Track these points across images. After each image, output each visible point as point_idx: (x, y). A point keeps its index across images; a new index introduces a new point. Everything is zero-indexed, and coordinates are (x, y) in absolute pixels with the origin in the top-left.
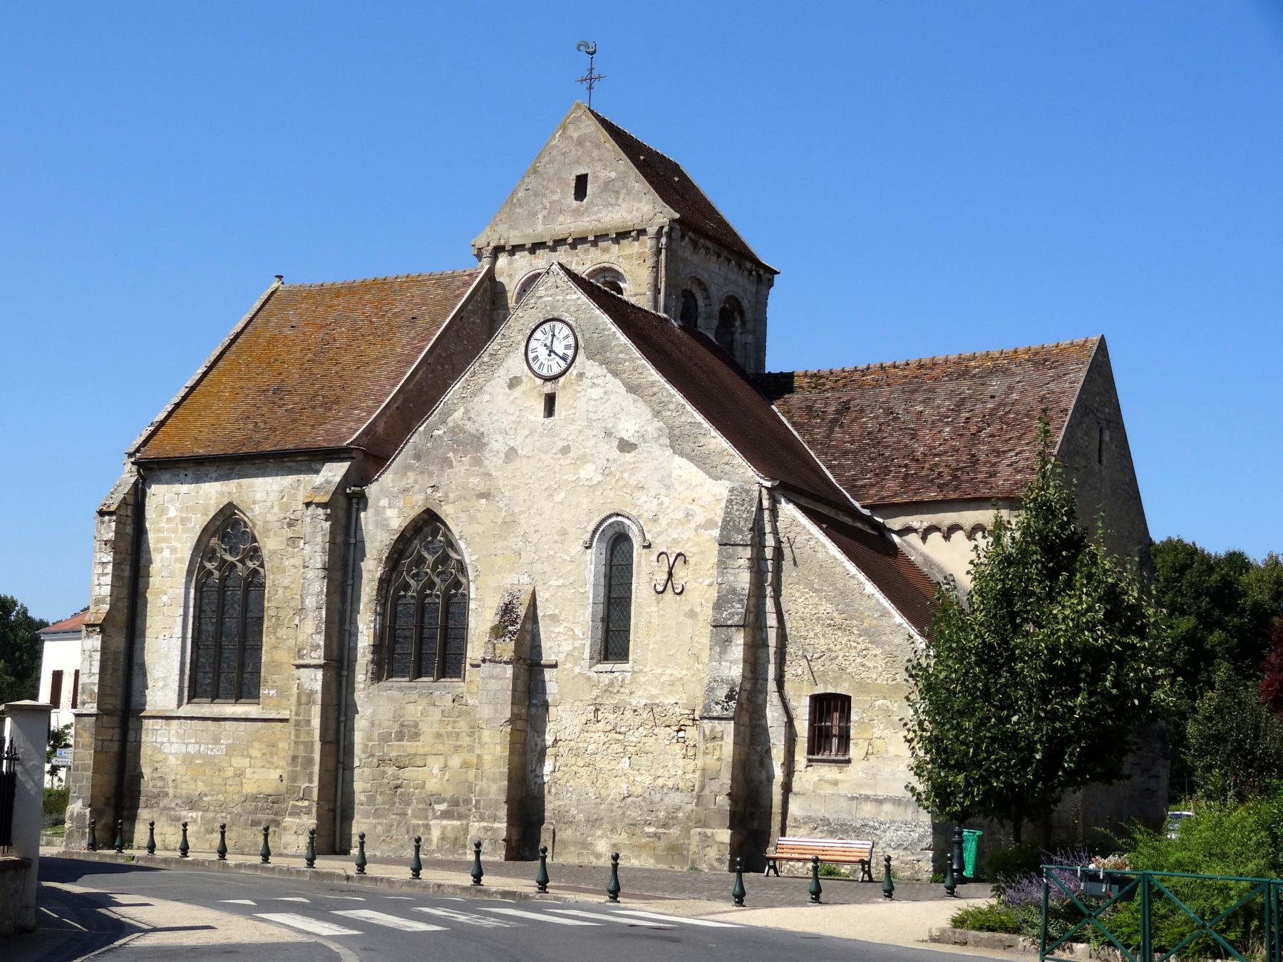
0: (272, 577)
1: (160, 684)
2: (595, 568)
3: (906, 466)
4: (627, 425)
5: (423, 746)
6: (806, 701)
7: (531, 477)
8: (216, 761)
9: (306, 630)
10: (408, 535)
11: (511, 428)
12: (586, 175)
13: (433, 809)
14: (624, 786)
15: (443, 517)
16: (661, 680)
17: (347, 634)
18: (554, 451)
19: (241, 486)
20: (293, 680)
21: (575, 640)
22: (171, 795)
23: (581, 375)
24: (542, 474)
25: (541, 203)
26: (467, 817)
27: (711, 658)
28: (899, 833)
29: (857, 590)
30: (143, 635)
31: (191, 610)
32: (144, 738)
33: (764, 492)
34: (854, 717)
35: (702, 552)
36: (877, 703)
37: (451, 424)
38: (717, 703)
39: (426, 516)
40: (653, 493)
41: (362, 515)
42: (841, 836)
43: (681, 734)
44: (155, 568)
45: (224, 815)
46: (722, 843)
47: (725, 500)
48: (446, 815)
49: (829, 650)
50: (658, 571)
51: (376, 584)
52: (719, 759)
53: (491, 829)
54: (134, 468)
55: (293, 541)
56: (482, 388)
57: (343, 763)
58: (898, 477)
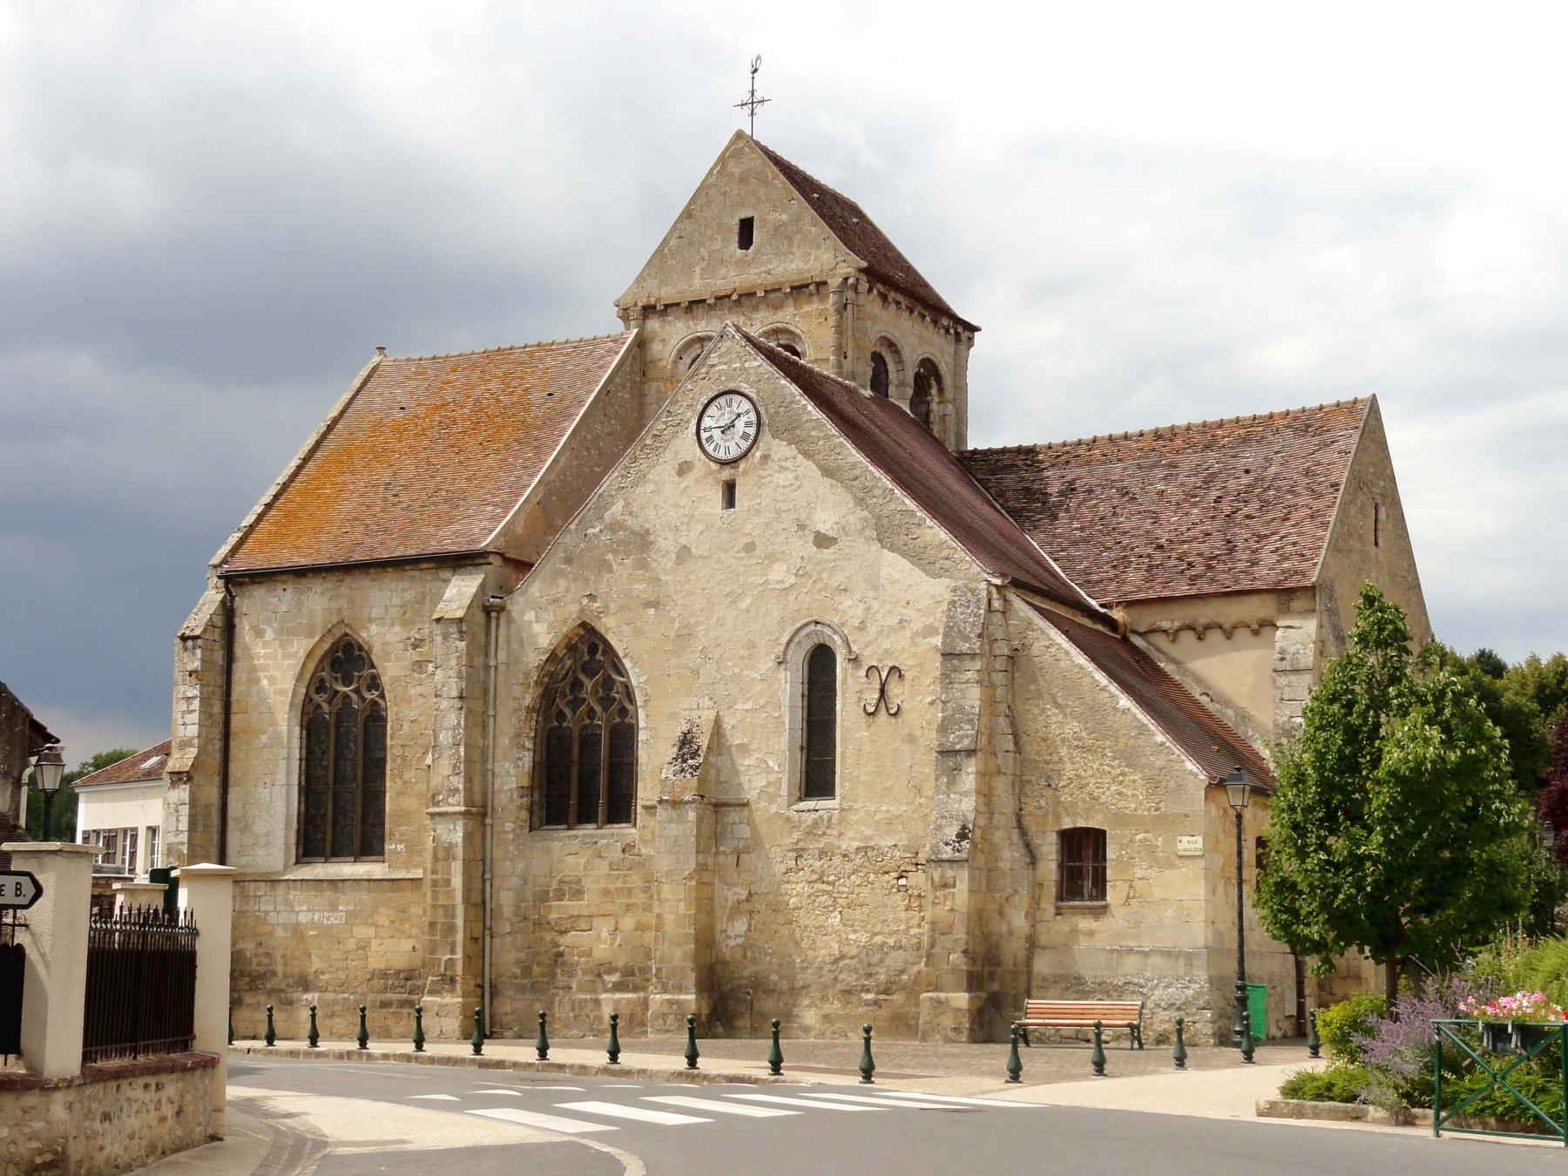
2: (791, 687)
3: (1149, 556)
4: (825, 516)
5: (588, 906)
6: (1053, 838)
7: (708, 581)
9: (441, 771)
10: (561, 655)
11: (683, 523)
12: (752, 219)
13: (603, 981)
14: (836, 946)
15: (602, 631)
16: (876, 818)
17: (490, 774)
18: (736, 549)
20: (426, 831)
21: (768, 773)
22: (280, 974)
23: (765, 458)
24: (723, 577)
25: (698, 253)
26: (645, 989)
27: (937, 790)
28: (1170, 990)
29: (1109, 705)
33: (994, 590)
34: (1110, 854)
35: (921, 665)
36: (1138, 837)
38: (947, 844)
39: (582, 632)
40: (858, 596)
42: (1100, 996)
43: (902, 882)
45: (346, 996)
46: (959, 1010)
47: (946, 602)
48: (618, 987)
49: (1078, 776)
50: (867, 689)
52: (952, 910)
53: (677, 1002)
54: (221, 583)
55: (419, 665)
56: (645, 476)
57: (491, 929)
58: (1140, 569)
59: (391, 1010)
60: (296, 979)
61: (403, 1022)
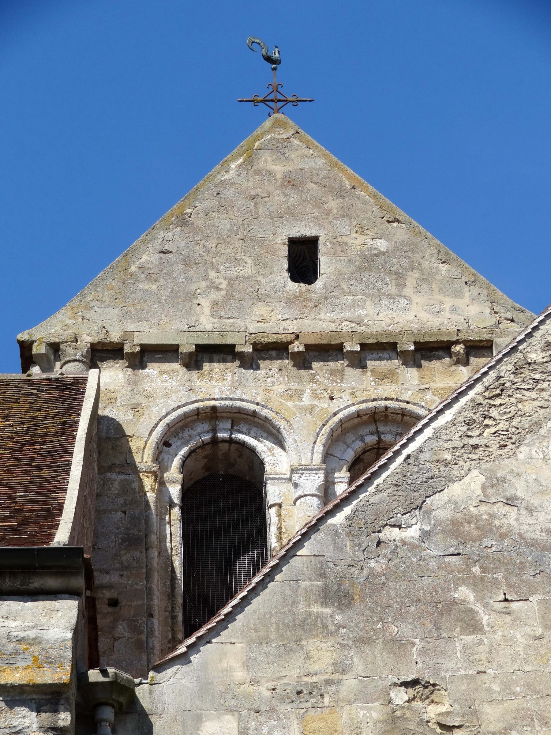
37: (443, 514)
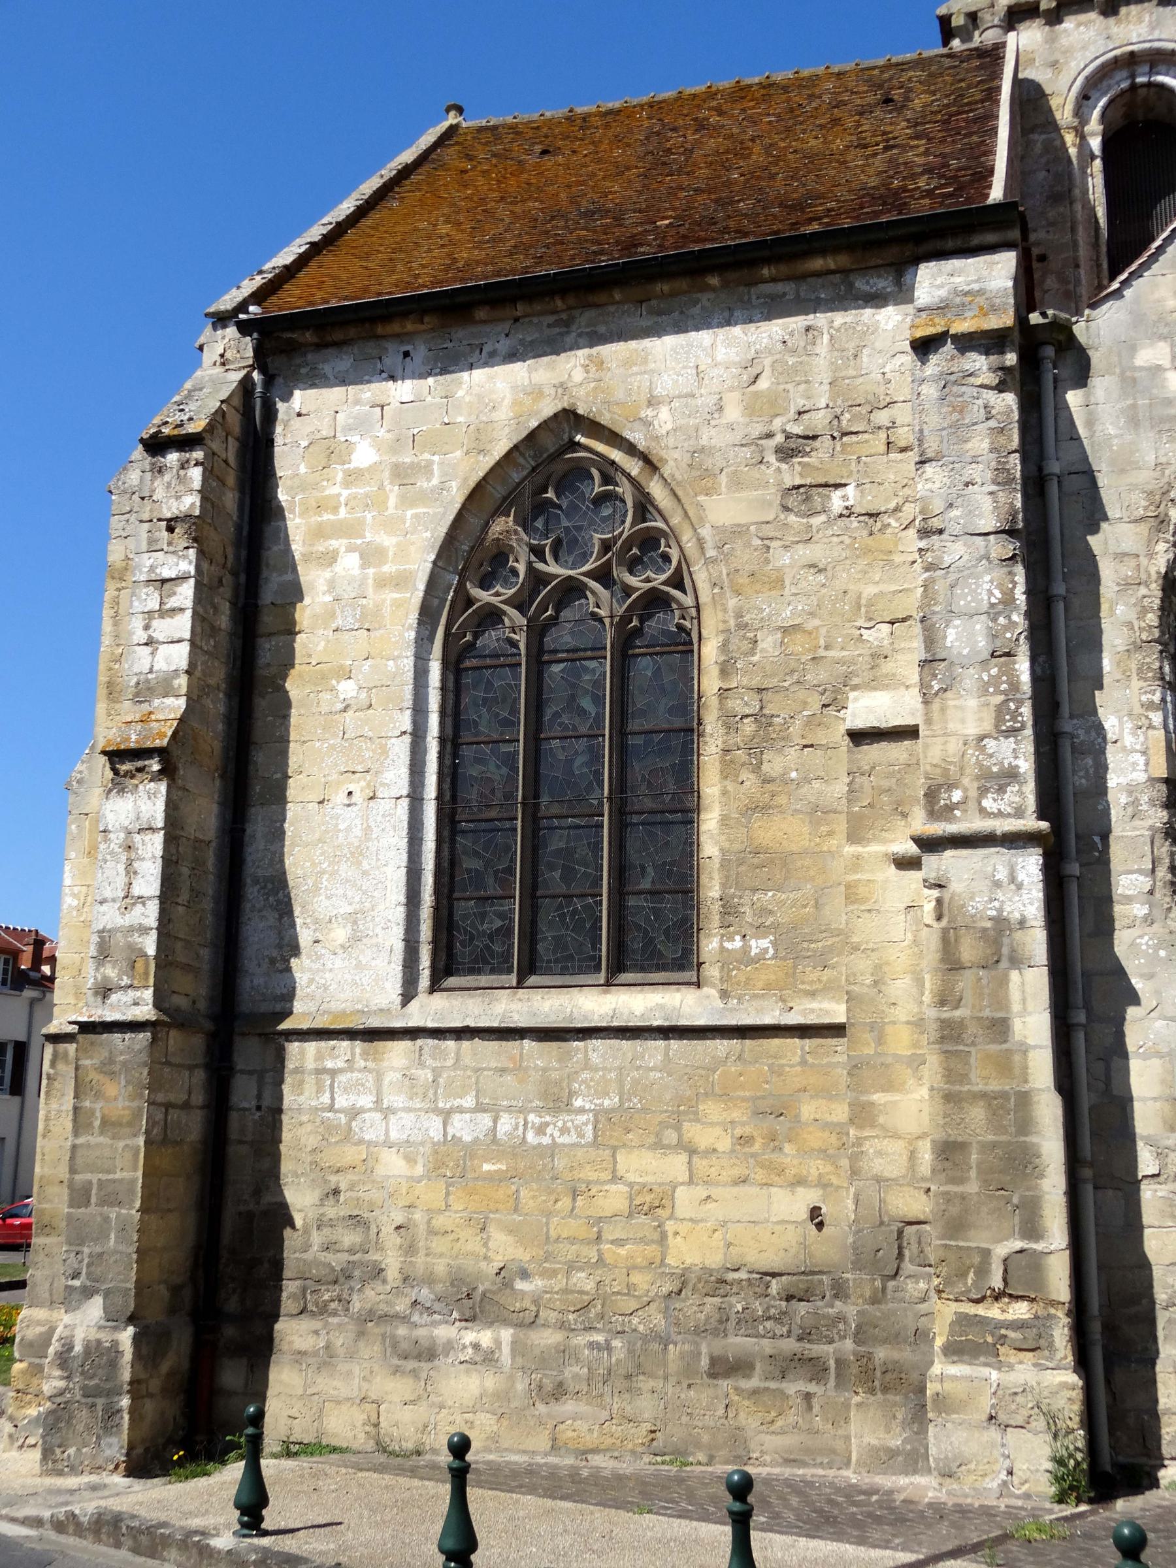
0: (732, 602)
1: (340, 934)
8: (560, 1163)
19: (600, 364)
22: (392, 1274)
30: (278, 796)
31: (434, 721)
32: (289, 1097)
41: (1073, 398)
44: (304, 614)
51: (1153, 594)
59: (754, 1382)
60: (439, 1288)
61: (791, 1417)
